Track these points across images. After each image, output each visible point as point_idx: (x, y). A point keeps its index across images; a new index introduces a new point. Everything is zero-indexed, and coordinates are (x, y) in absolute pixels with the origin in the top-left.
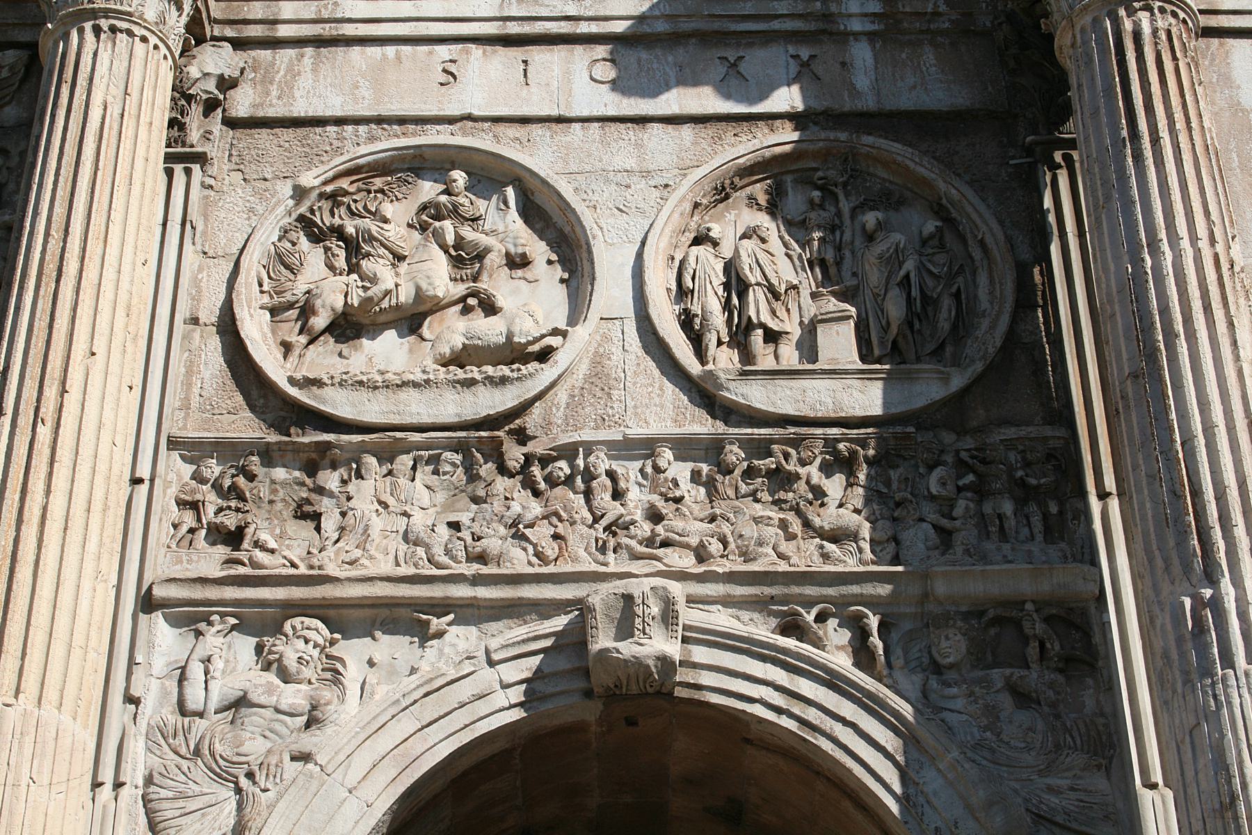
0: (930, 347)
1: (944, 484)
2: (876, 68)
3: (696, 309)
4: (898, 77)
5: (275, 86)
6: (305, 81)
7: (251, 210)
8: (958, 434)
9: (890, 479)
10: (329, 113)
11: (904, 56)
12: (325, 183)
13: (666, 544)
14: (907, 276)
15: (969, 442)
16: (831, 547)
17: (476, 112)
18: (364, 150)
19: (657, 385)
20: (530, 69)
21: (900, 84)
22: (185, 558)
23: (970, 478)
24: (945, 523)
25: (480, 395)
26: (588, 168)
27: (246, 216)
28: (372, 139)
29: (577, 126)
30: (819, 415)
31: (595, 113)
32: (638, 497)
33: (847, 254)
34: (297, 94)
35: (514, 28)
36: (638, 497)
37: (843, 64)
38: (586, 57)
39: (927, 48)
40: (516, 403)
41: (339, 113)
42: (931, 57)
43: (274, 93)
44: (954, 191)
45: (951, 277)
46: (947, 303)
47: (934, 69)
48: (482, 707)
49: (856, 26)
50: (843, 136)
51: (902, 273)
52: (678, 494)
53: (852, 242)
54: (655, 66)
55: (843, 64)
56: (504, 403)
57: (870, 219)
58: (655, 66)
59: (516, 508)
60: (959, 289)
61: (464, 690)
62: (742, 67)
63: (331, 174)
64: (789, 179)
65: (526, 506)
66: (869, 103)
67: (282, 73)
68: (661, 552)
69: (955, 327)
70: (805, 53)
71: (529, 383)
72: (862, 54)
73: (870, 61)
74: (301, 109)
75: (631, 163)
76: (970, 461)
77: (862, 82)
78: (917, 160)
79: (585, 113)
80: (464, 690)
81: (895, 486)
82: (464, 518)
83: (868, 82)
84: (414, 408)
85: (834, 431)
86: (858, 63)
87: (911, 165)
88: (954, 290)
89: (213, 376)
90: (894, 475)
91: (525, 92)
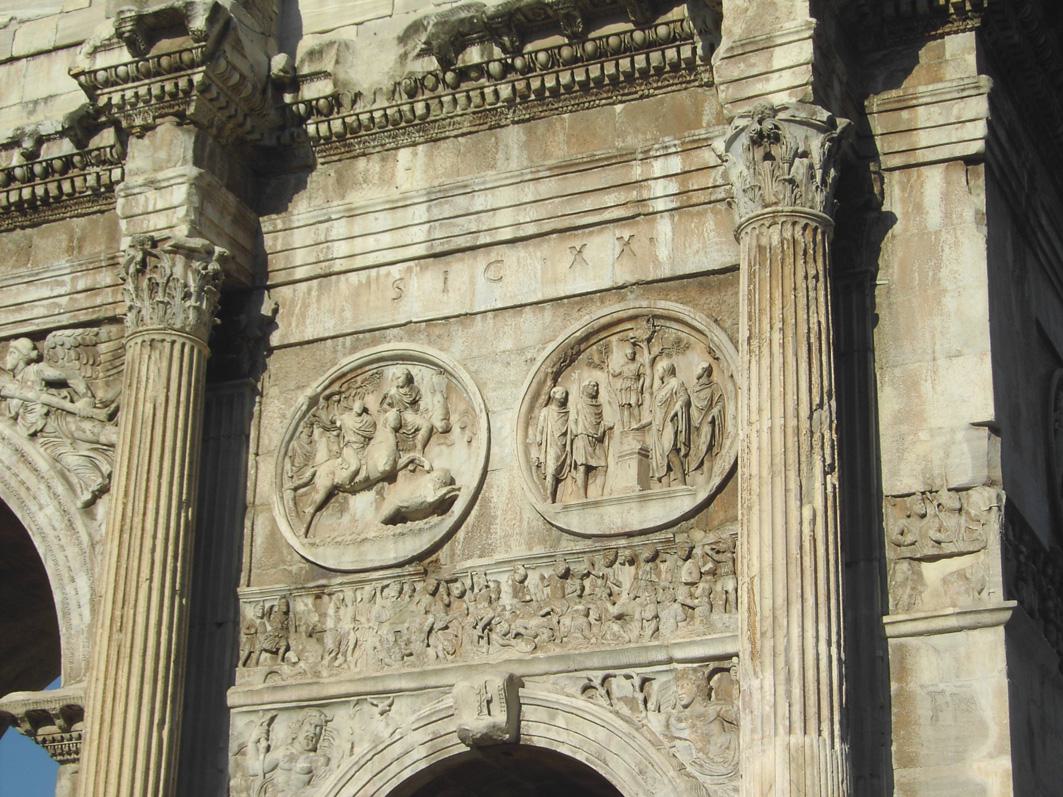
0: (694, 465)
1: (690, 573)
2: (673, 239)
3: (542, 460)
4: (687, 245)
5: (295, 318)
6: (312, 311)
7: (284, 416)
8: (705, 531)
9: (660, 571)
10: (326, 335)
11: (693, 225)
12: (325, 389)
13: (518, 635)
14: (676, 415)
15: (712, 537)
16: (616, 627)
17: (414, 320)
18: (345, 361)
19: (518, 518)
20: (451, 277)
21: (688, 251)
22: (246, 674)
23: (710, 565)
24: (689, 602)
25: (407, 543)
26: (484, 352)
27: (279, 420)
28: (354, 349)
29: (479, 317)
30: (613, 532)
31: (489, 308)
32: (507, 599)
33: (647, 395)
34: (308, 321)
35: (438, 249)
36: (507, 599)
37: (651, 239)
38: (484, 262)
39: (710, 216)
40: (429, 546)
41: (332, 334)
42: (711, 223)
43: (294, 324)
44: (715, 338)
45: (710, 406)
46: (706, 430)
47: (712, 234)
48: (407, 760)
49: (660, 205)
50: (644, 303)
51: (672, 413)
52: (528, 598)
53: (651, 387)
54: (529, 261)
55: (651, 239)
56: (421, 547)
57: (662, 365)
58: (529, 261)
59: (430, 619)
60: (713, 417)
61: (397, 749)
62: (586, 253)
63: (327, 382)
64: (614, 339)
65: (438, 617)
66: (667, 273)
67: (299, 306)
68: (513, 642)
69: (710, 447)
70: (626, 236)
71: (437, 530)
72: (664, 227)
73: (670, 234)
74: (308, 336)
75: (507, 344)
76: (710, 553)
77: (663, 253)
78: (692, 315)
79: (483, 309)
80: (397, 749)
81: (663, 576)
82: (403, 627)
83: (667, 253)
84: (369, 557)
85: (623, 542)
86: (661, 238)
87: (689, 320)
88: (710, 419)
89: (262, 543)
90: (663, 567)
91: (445, 298)
